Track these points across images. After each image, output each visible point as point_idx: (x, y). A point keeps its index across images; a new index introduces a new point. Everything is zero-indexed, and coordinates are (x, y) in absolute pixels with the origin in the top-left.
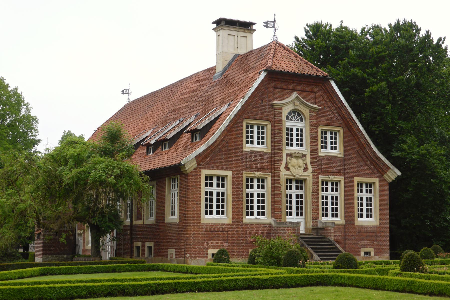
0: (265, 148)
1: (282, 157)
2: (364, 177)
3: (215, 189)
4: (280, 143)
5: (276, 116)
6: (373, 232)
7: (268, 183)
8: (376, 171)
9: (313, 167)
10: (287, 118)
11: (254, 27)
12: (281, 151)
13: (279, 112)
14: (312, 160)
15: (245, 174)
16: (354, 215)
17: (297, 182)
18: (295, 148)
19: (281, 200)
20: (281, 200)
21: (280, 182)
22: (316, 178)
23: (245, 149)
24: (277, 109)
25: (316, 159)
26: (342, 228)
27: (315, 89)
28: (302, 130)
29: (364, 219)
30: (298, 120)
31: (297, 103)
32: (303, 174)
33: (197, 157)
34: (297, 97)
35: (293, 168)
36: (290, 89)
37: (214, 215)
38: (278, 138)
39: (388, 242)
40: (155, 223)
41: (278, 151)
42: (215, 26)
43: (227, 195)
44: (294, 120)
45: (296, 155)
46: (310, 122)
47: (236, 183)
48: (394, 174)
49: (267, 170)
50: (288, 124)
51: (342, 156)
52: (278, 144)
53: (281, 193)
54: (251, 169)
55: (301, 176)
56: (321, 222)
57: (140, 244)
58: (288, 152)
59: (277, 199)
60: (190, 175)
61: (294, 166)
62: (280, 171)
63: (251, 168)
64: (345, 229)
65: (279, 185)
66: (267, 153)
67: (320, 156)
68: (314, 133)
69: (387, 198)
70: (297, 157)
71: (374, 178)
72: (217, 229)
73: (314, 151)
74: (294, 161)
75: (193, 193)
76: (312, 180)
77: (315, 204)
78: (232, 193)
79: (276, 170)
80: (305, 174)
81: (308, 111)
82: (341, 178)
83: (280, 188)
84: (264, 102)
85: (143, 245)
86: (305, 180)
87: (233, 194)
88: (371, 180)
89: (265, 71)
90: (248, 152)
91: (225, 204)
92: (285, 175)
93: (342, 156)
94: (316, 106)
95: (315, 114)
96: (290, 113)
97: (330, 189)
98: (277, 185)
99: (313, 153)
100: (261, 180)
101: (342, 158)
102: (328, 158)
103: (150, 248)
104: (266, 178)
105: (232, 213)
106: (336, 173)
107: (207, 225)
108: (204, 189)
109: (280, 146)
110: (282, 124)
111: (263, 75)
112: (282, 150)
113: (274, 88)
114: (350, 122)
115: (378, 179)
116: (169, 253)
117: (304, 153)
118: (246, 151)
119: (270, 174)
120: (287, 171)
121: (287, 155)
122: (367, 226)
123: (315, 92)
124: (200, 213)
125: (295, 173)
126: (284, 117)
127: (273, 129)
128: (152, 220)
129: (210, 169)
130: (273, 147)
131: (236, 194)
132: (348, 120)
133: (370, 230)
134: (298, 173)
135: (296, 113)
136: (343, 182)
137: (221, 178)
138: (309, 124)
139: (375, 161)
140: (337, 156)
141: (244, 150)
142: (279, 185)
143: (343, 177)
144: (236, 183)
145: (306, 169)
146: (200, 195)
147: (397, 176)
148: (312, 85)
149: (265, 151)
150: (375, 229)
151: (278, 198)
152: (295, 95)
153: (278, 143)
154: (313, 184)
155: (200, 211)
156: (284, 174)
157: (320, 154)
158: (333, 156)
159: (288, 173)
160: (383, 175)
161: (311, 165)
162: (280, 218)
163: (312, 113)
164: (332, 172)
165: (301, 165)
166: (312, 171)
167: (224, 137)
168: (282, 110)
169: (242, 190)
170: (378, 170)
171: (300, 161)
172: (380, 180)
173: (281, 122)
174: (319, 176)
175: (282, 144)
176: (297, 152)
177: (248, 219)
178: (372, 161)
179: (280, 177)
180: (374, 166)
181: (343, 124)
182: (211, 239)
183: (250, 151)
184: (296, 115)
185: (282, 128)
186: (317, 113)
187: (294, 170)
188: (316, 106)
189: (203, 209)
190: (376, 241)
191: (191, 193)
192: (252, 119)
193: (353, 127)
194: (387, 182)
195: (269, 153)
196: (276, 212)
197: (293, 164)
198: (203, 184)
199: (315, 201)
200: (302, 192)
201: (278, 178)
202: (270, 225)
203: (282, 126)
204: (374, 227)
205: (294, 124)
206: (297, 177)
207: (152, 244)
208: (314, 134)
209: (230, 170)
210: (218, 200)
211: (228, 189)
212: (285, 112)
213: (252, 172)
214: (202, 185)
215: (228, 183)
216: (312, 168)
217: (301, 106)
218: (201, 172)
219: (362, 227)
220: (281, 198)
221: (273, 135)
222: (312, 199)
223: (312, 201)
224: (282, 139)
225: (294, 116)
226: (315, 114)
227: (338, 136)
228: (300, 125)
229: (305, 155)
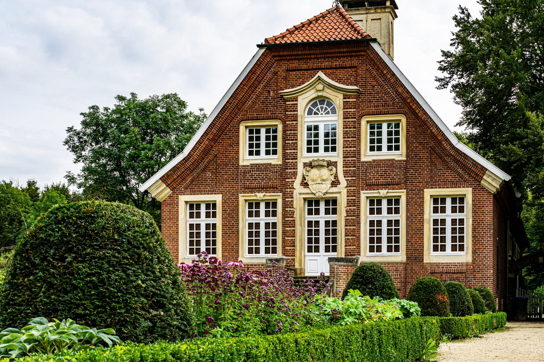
0: (276, 160)
1: (297, 169)
2: (444, 188)
4: (294, 149)
5: (288, 111)
6: (461, 273)
9: (348, 178)
10: (310, 112)
12: (296, 161)
13: (292, 104)
14: (346, 169)
16: (423, 248)
17: (327, 202)
19: (295, 230)
20: (295, 230)
21: (293, 205)
23: (243, 162)
24: (289, 101)
25: (354, 167)
26: (401, 268)
27: (355, 62)
30: (328, 113)
31: (320, 87)
32: (330, 191)
35: (313, 183)
36: (313, 69)
38: (290, 142)
41: (291, 161)
44: (322, 114)
45: (316, 163)
47: (227, 210)
48: (495, 178)
49: (277, 189)
50: (311, 120)
51: (404, 158)
52: (290, 151)
53: (294, 220)
54: (252, 190)
55: (326, 193)
58: (307, 161)
59: (288, 229)
60: (164, 204)
61: (313, 181)
62: (293, 188)
63: (252, 188)
64: (406, 269)
65: (292, 209)
66: (277, 165)
67: (363, 162)
68: (350, 128)
71: (464, 187)
74: (314, 172)
75: (168, 227)
76: (346, 198)
78: (223, 224)
79: (287, 188)
80: (334, 190)
81: (341, 96)
82: (402, 194)
83: (293, 212)
84: (272, 94)
88: (456, 191)
90: (248, 166)
92: (300, 194)
93: (404, 159)
94: (355, 87)
95: (355, 100)
96: (315, 105)
98: (289, 209)
99: (349, 159)
101: (404, 161)
102: (376, 164)
104: (400, 196)
105: (222, 250)
106: (394, 185)
109: (293, 153)
110: (297, 120)
112: (297, 159)
113: (287, 70)
114: (411, 104)
115: (470, 190)
117: (333, 160)
118: (245, 166)
119: (281, 194)
120: (304, 187)
121: (305, 165)
122: (448, 264)
123: (356, 67)
124: (178, 253)
125: (315, 190)
127: (284, 131)
129: (191, 194)
131: (228, 226)
132: (408, 101)
133: (453, 269)
138: (342, 116)
140: (393, 160)
141: (241, 163)
142: (292, 209)
143: (405, 191)
144: (227, 210)
145: (335, 183)
146: (178, 229)
147: (501, 181)
148: (351, 56)
149: (274, 162)
150: (464, 268)
151: (290, 227)
153: (290, 149)
154: (347, 204)
157: (363, 159)
158: (387, 160)
159: (306, 190)
160: (480, 182)
161: (345, 177)
162: (292, 256)
163: (349, 98)
164: (384, 185)
165: (324, 178)
166: (346, 185)
168: (297, 101)
169: (238, 220)
171: (325, 173)
172: (474, 190)
173: (295, 118)
174: (362, 192)
175: (297, 149)
176: (316, 159)
178: (457, 161)
179: (292, 198)
180: (463, 170)
181: (406, 109)
183: (251, 164)
184: (325, 106)
185: (297, 128)
186: (357, 97)
187: (314, 185)
188: (355, 87)
191: (166, 227)
192: (253, 119)
193: (417, 111)
194: (490, 192)
195: (280, 165)
197: (312, 177)
199: (351, 229)
200: (336, 217)
201: (290, 199)
203: (297, 124)
204: (462, 264)
206: (319, 195)
208: (351, 129)
209: (219, 194)
210: (208, 235)
213: (253, 194)
214: (179, 216)
216: (346, 180)
217: (328, 91)
218: (178, 198)
219: (438, 265)
220: (294, 227)
221: (284, 139)
222: (346, 226)
223: (346, 229)
224: (297, 143)
225: (322, 108)
226: (355, 100)
229: (336, 162)
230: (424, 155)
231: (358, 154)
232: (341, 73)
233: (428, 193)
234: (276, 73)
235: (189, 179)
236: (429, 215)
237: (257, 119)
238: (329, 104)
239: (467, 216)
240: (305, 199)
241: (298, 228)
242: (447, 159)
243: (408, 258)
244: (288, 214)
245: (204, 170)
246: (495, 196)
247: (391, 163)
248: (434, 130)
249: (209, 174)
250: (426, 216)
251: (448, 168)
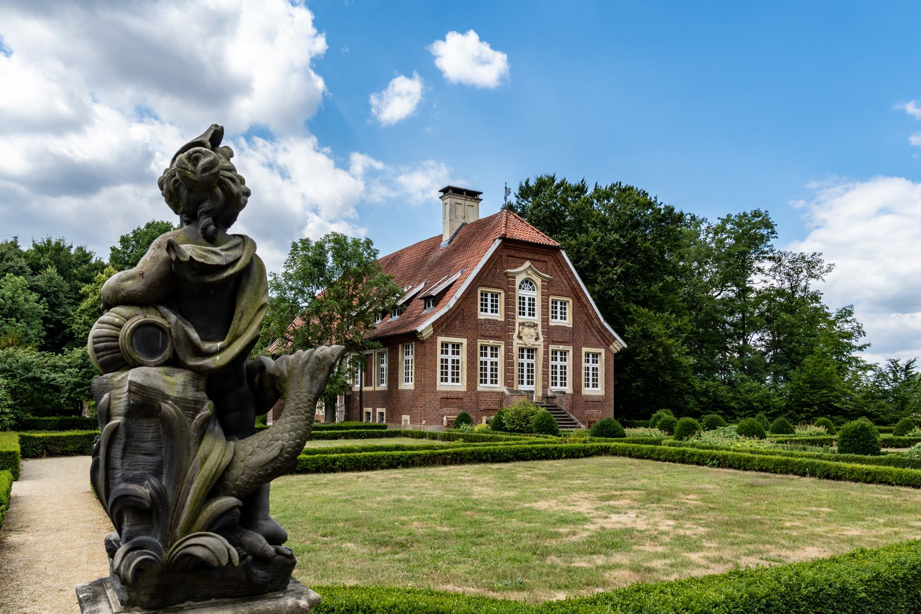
0: (500, 316)
3: (450, 357)
7: (501, 352)
8: (602, 342)
11: (480, 197)
15: (480, 342)
17: (528, 350)
22: (546, 347)
27: (546, 259)
28: (534, 300)
31: (530, 272)
33: (433, 324)
34: (530, 266)
37: (450, 382)
39: (613, 411)
40: (387, 389)
43: (462, 362)
46: (542, 292)
56: (551, 391)
57: (370, 410)
58: (521, 321)
61: (526, 336)
64: (573, 398)
69: (612, 369)
70: (529, 326)
72: (452, 396)
73: (545, 320)
74: (526, 330)
80: (537, 343)
81: (540, 280)
85: (374, 411)
86: (536, 349)
87: (468, 362)
89: (500, 238)
91: (460, 371)
96: (522, 282)
97: (559, 359)
100: (495, 349)
102: (557, 328)
103: (382, 414)
107: (442, 392)
108: (440, 356)
111: (498, 242)
116: (403, 419)
121: (520, 324)
126: (517, 287)
127: (506, 298)
128: (384, 386)
130: (507, 316)
133: (596, 399)
135: (528, 282)
136: (571, 352)
137: (456, 346)
139: (602, 332)
145: (537, 339)
149: (499, 319)
152: (528, 264)
155: (436, 378)
159: (521, 342)
167: (460, 305)
170: (604, 341)
171: (532, 330)
177: (481, 387)
178: (599, 332)
182: (447, 406)
186: (548, 282)
189: (439, 376)
190: (602, 410)
196: (508, 382)
198: (439, 352)
202: (503, 393)
204: (600, 396)
205: (526, 293)
206: (529, 346)
207: (384, 410)
211: (463, 357)
212: (518, 280)
215: (464, 350)
219: (588, 396)
221: (507, 303)
227: (567, 306)
228: (533, 294)
230: (582, 325)
231: (548, 321)
232: (538, 264)
234: (501, 256)
236: (584, 365)
237: (490, 287)
239: (601, 366)
242: (593, 329)
243: (574, 391)
246: (616, 355)
248: (591, 311)
249: (457, 322)
251: (594, 335)
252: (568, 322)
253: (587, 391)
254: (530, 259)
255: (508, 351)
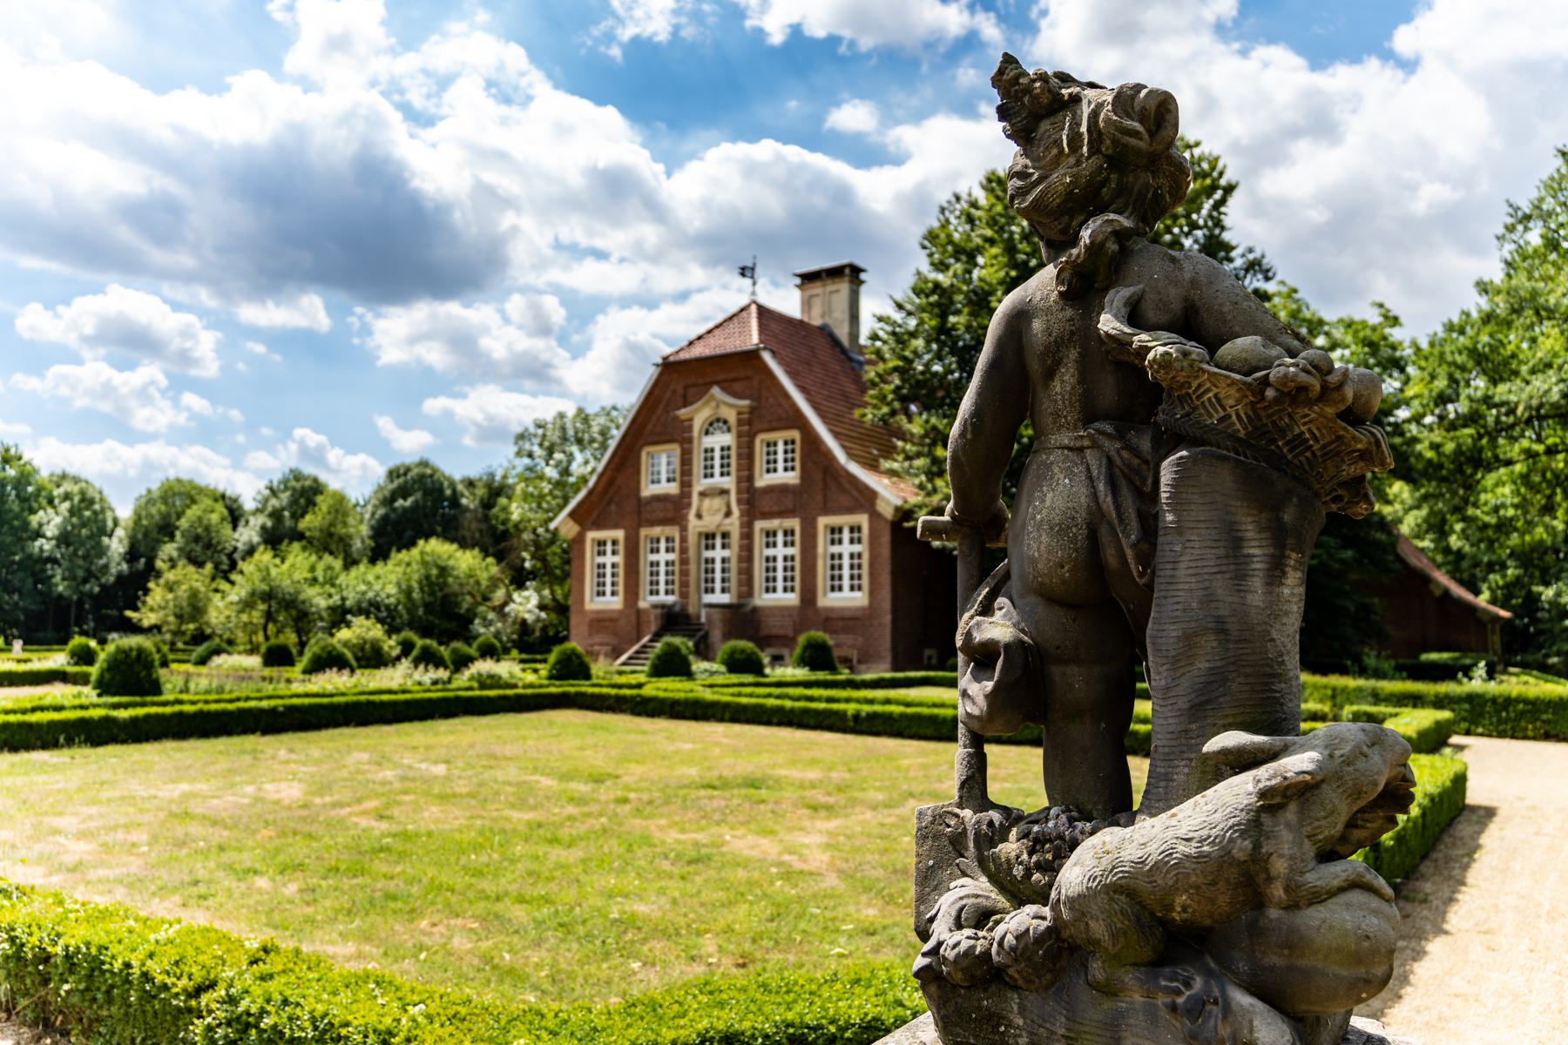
0: (673, 489)
10: (707, 433)
18: (718, 481)
29: (846, 593)
37: (608, 597)
42: (798, 281)
50: (708, 441)
54: (652, 523)
73: (746, 479)
74: (707, 503)
77: (684, 573)
80: (727, 521)
82: (794, 523)
117: (726, 486)
121: (703, 494)
122: (842, 609)
126: (696, 433)
134: (711, 521)
145: (728, 514)
156: (694, 525)
171: (718, 503)
173: (690, 440)
204: (857, 609)
205: (721, 440)
206: (711, 528)
212: (698, 424)
219: (832, 609)
231: (750, 478)
232: (737, 386)
233: (823, 522)
235: (595, 514)
238: (725, 422)
240: (700, 534)
241: (693, 567)
244: (684, 550)
245: (609, 504)
247: (783, 489)
249: (613, 508)
250: (820, 550)
252: (792, 478)
253: (829, 600)
254: (717, 383)
255: (684, 539)
